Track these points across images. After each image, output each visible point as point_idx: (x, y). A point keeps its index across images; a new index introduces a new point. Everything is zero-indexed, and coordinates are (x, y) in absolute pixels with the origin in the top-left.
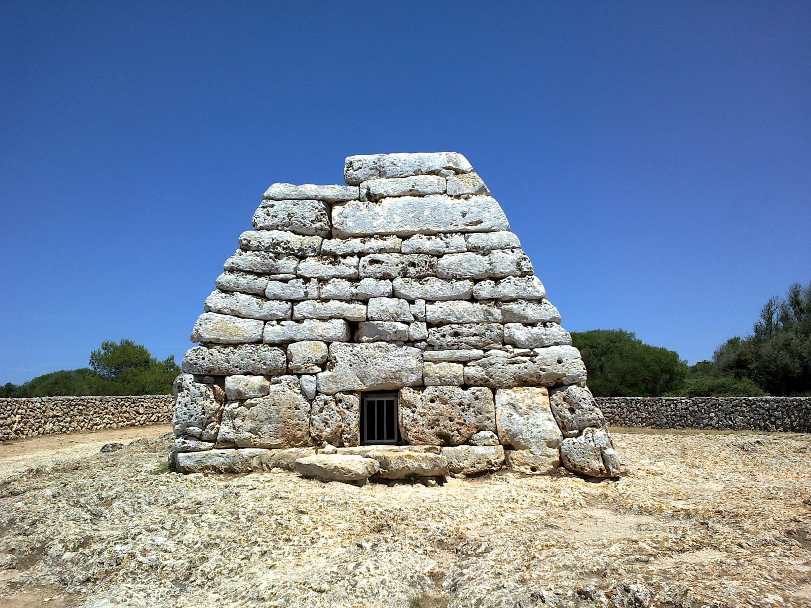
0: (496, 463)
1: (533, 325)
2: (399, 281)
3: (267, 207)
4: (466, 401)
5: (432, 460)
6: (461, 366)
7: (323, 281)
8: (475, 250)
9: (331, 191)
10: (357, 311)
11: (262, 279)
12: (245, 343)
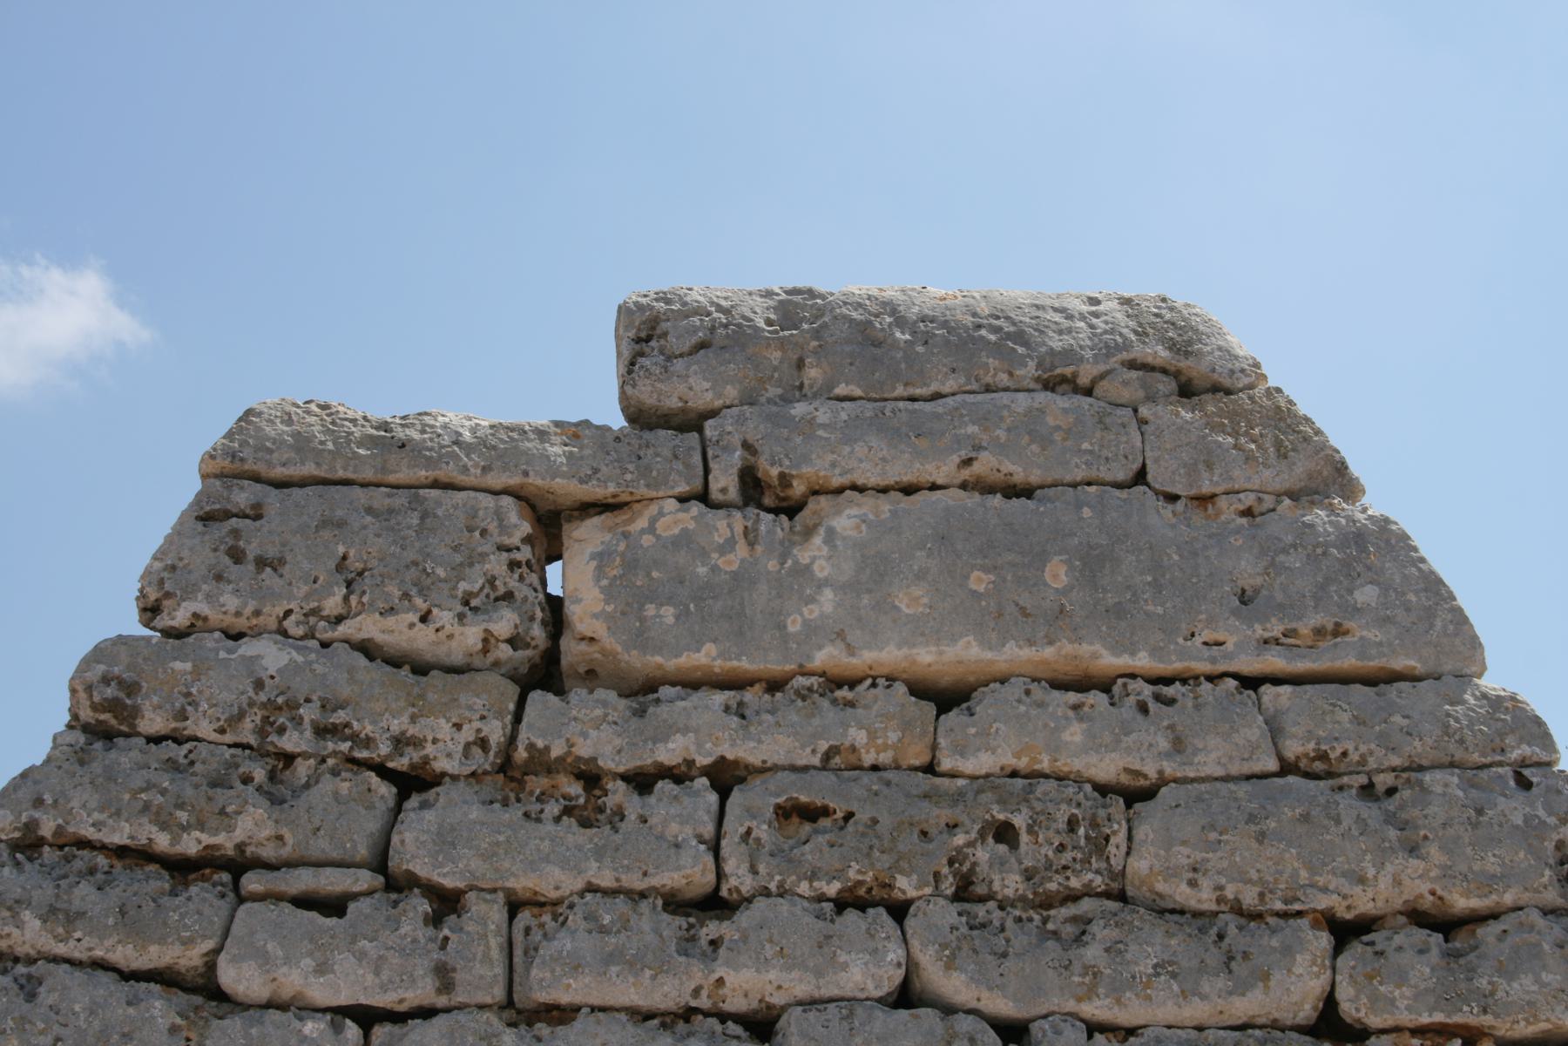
3: (227, 515)
8: (1319, 766)
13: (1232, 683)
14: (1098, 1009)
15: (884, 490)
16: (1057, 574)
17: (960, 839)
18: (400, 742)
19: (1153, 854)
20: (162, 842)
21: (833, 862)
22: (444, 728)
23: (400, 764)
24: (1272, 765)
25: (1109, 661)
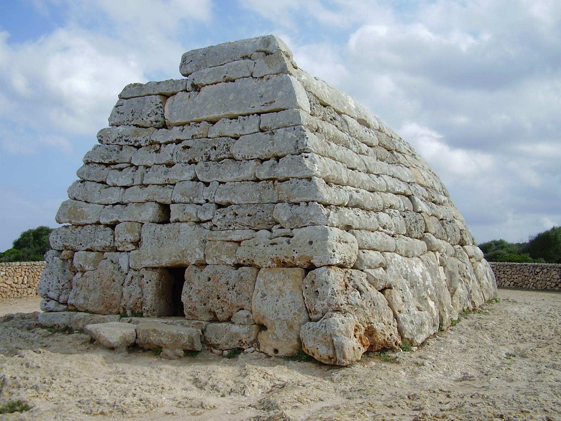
0: (246, 342)
5: (173, 336)
6: (236, 244)
10: (165, 195)
13: (256, 115)
14: (220, 179)
15: (212, 84)
16: (231, 97)
17: (207, 150)
18: (136, 142)
19: (237, 149)
20: (103, 161)
21: (186, 156)
22: (142, 139)
23: (136, 145)
24: (257, 130)
25: (236, 113)
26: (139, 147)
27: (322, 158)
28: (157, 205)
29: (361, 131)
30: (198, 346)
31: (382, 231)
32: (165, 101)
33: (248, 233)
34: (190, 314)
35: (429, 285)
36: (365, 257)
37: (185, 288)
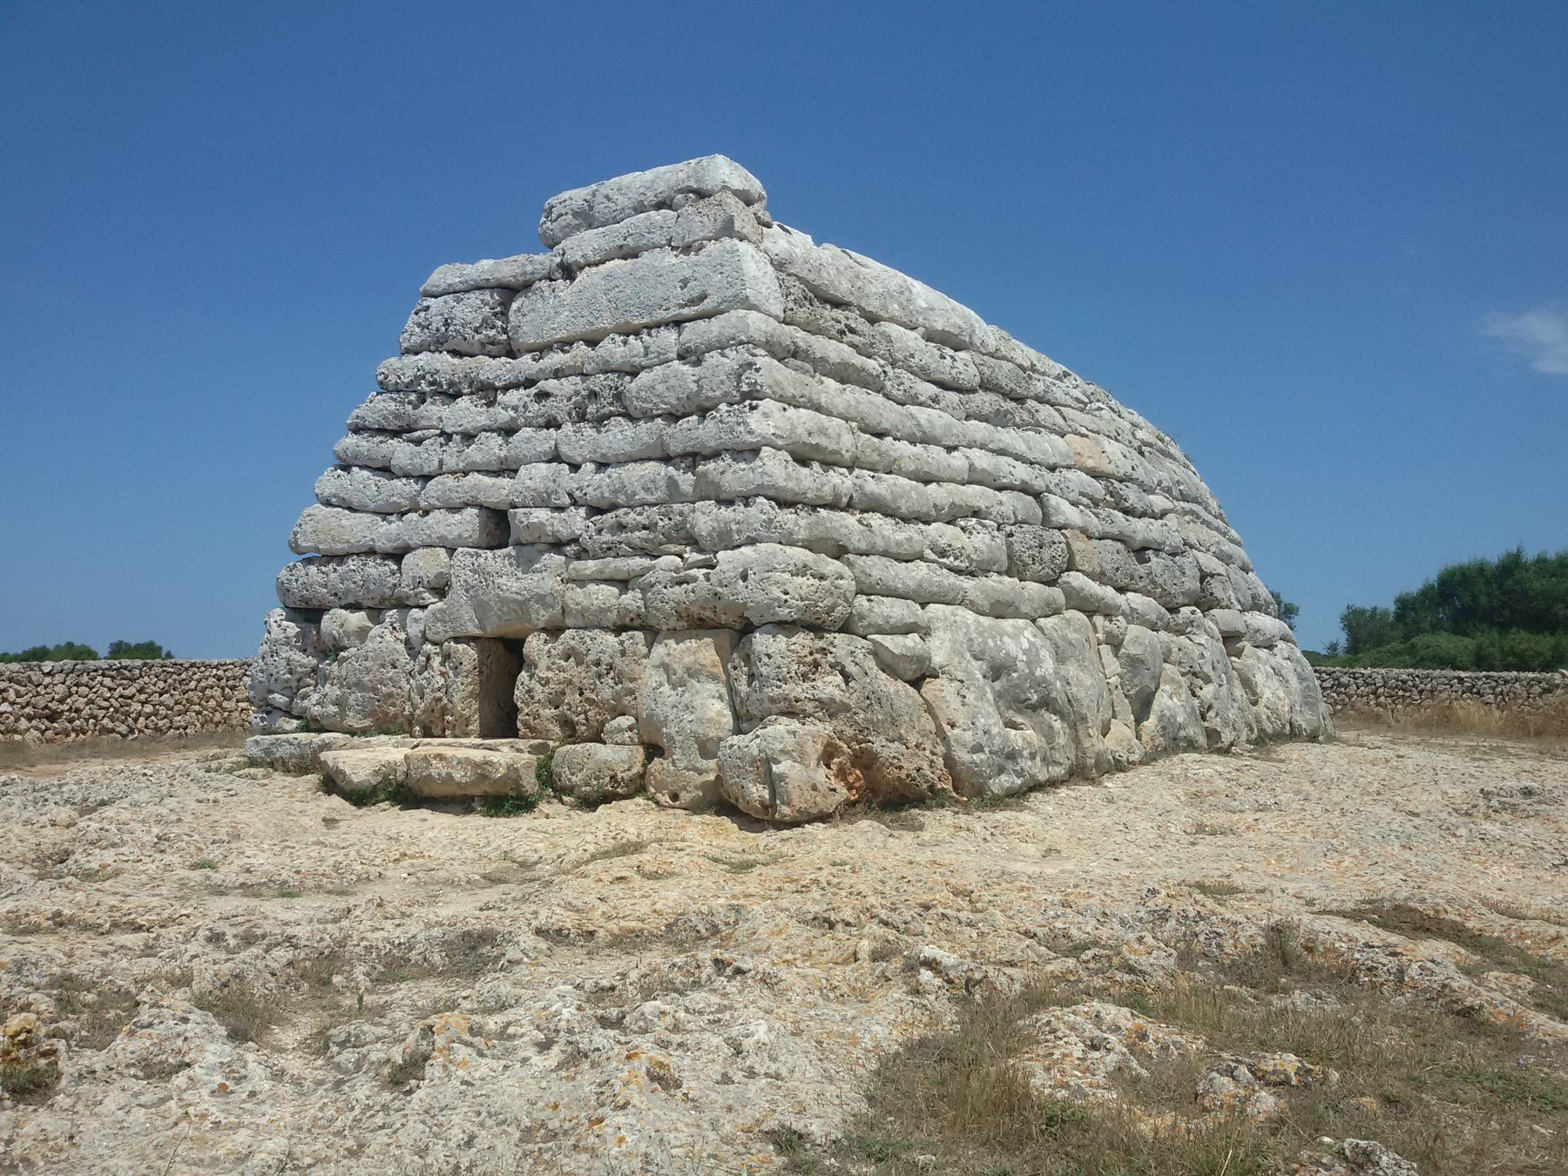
1: (730, 503)
2: (568, 428)
4: (606, 659)
5: (476, 765)
7: (468, 437)
9: (507, 268)
10: (498, 489)
11: (395, 442)
12: (349, 555)
18: (451, 384)
26: (458, 395)
27: (791, 411)
28: (484, 512)
29: (928, 354)
30: (530, 784)
31: (933, 561)
32: (512, 300)
33: (639, 562)
34: (527, 725)
35: (1044, 677)
36: (870, 610)
37: (524, 675)
